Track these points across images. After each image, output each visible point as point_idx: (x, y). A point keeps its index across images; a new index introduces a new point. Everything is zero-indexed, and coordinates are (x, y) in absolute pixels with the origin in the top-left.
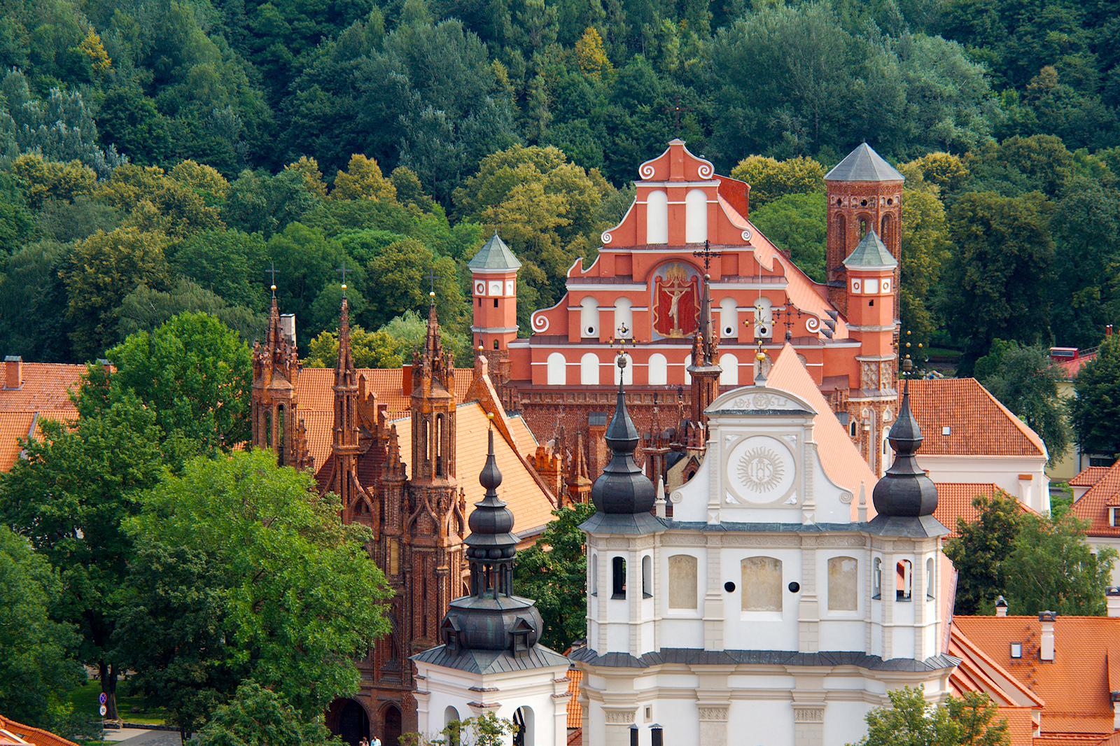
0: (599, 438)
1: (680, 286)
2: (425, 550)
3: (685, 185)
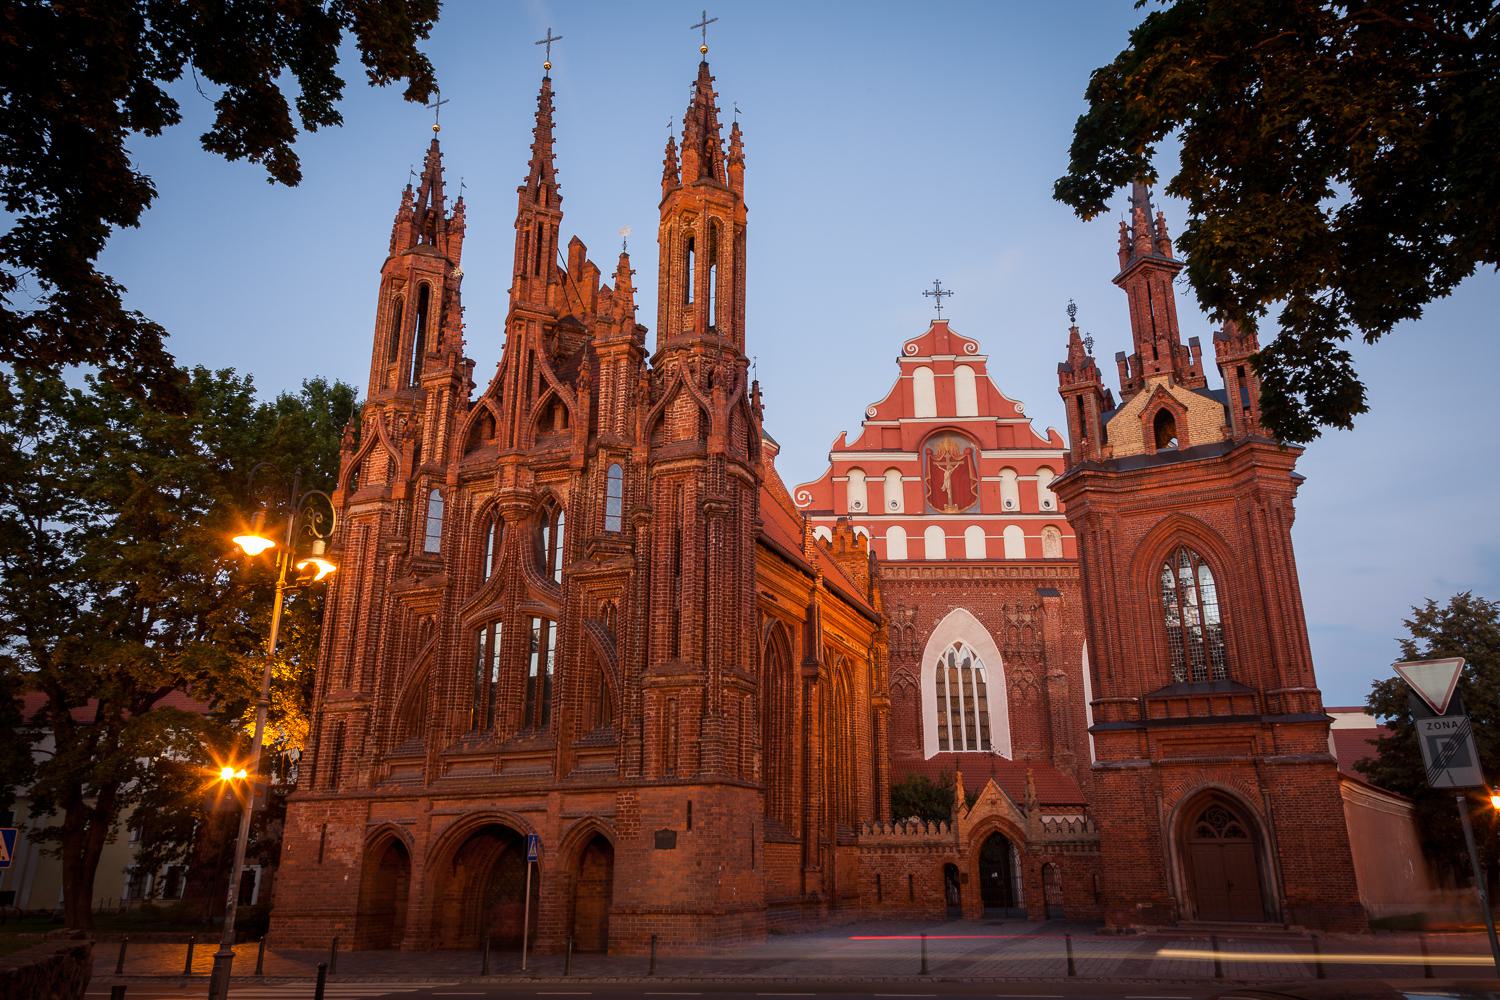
1: (951, 460)
2: (679, 465)
3: (951, 358)
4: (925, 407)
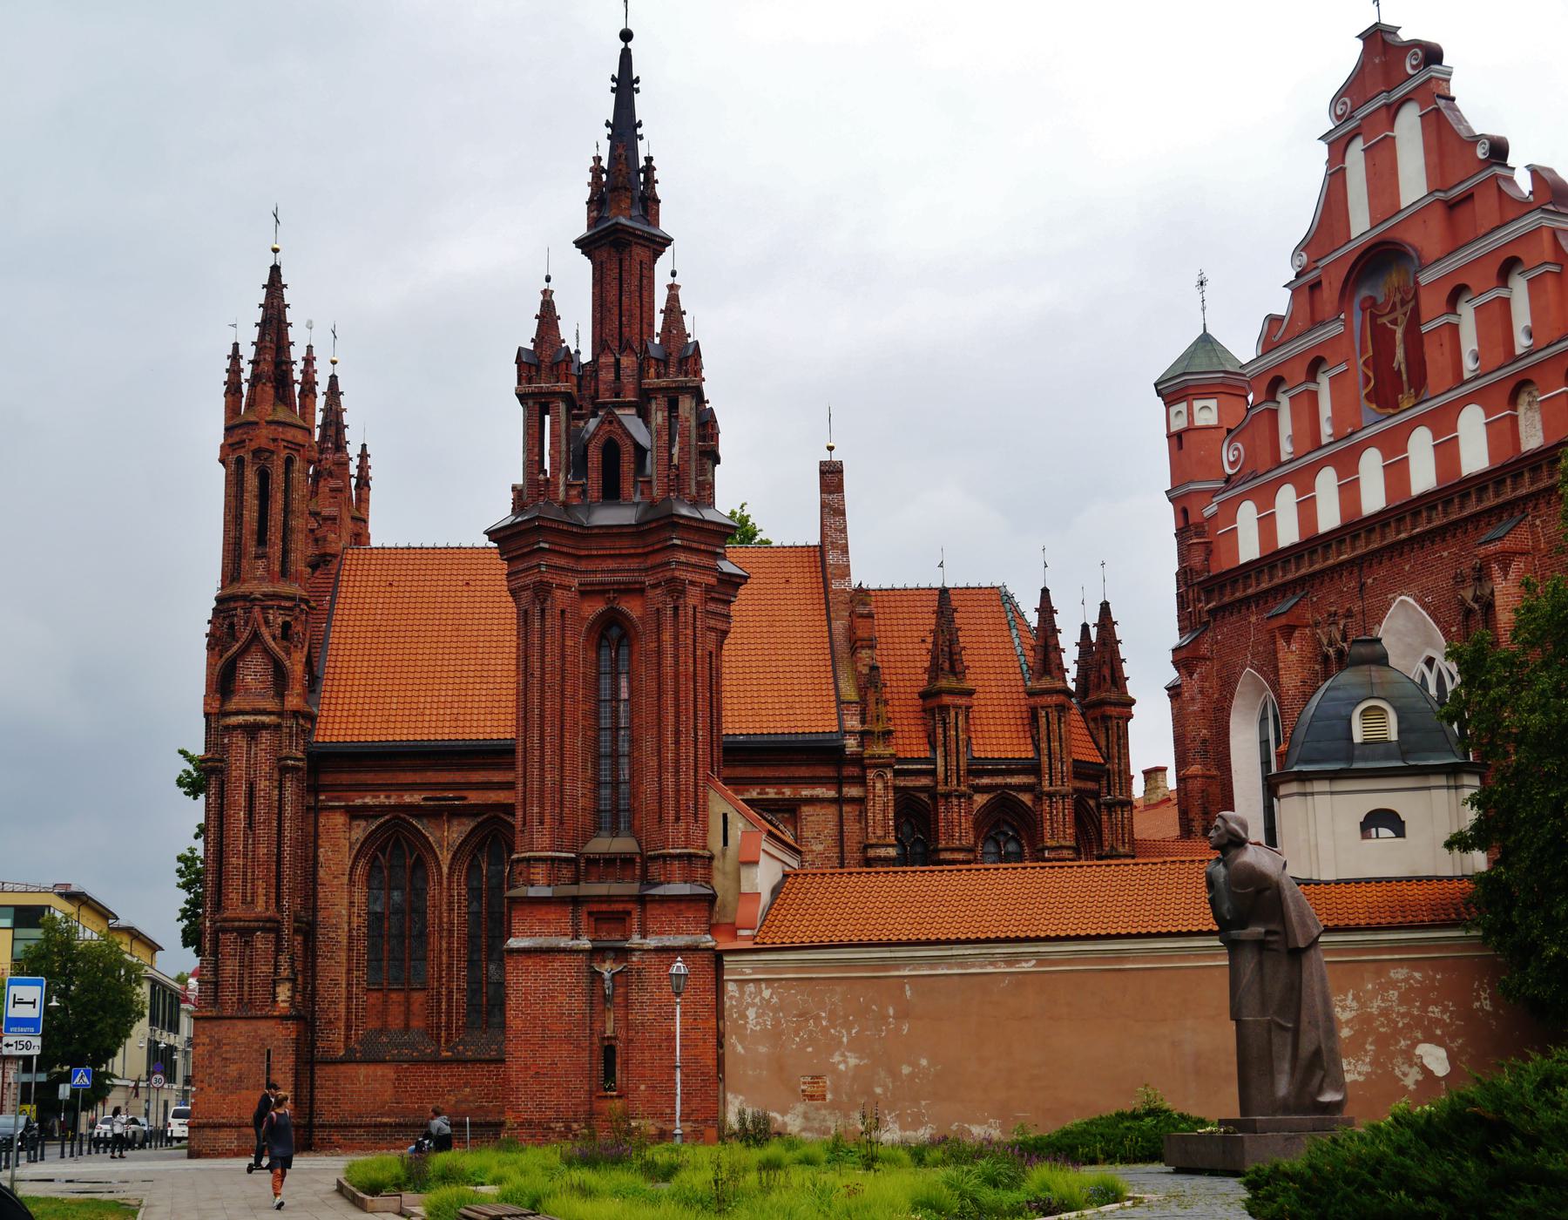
0: (1281, 643)
4: (1360, 223)
